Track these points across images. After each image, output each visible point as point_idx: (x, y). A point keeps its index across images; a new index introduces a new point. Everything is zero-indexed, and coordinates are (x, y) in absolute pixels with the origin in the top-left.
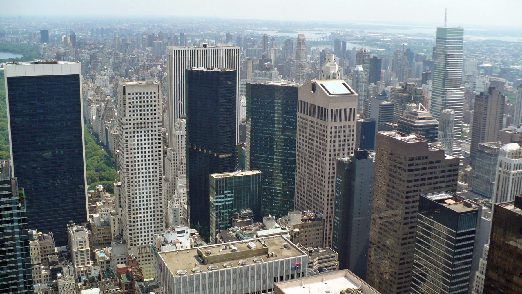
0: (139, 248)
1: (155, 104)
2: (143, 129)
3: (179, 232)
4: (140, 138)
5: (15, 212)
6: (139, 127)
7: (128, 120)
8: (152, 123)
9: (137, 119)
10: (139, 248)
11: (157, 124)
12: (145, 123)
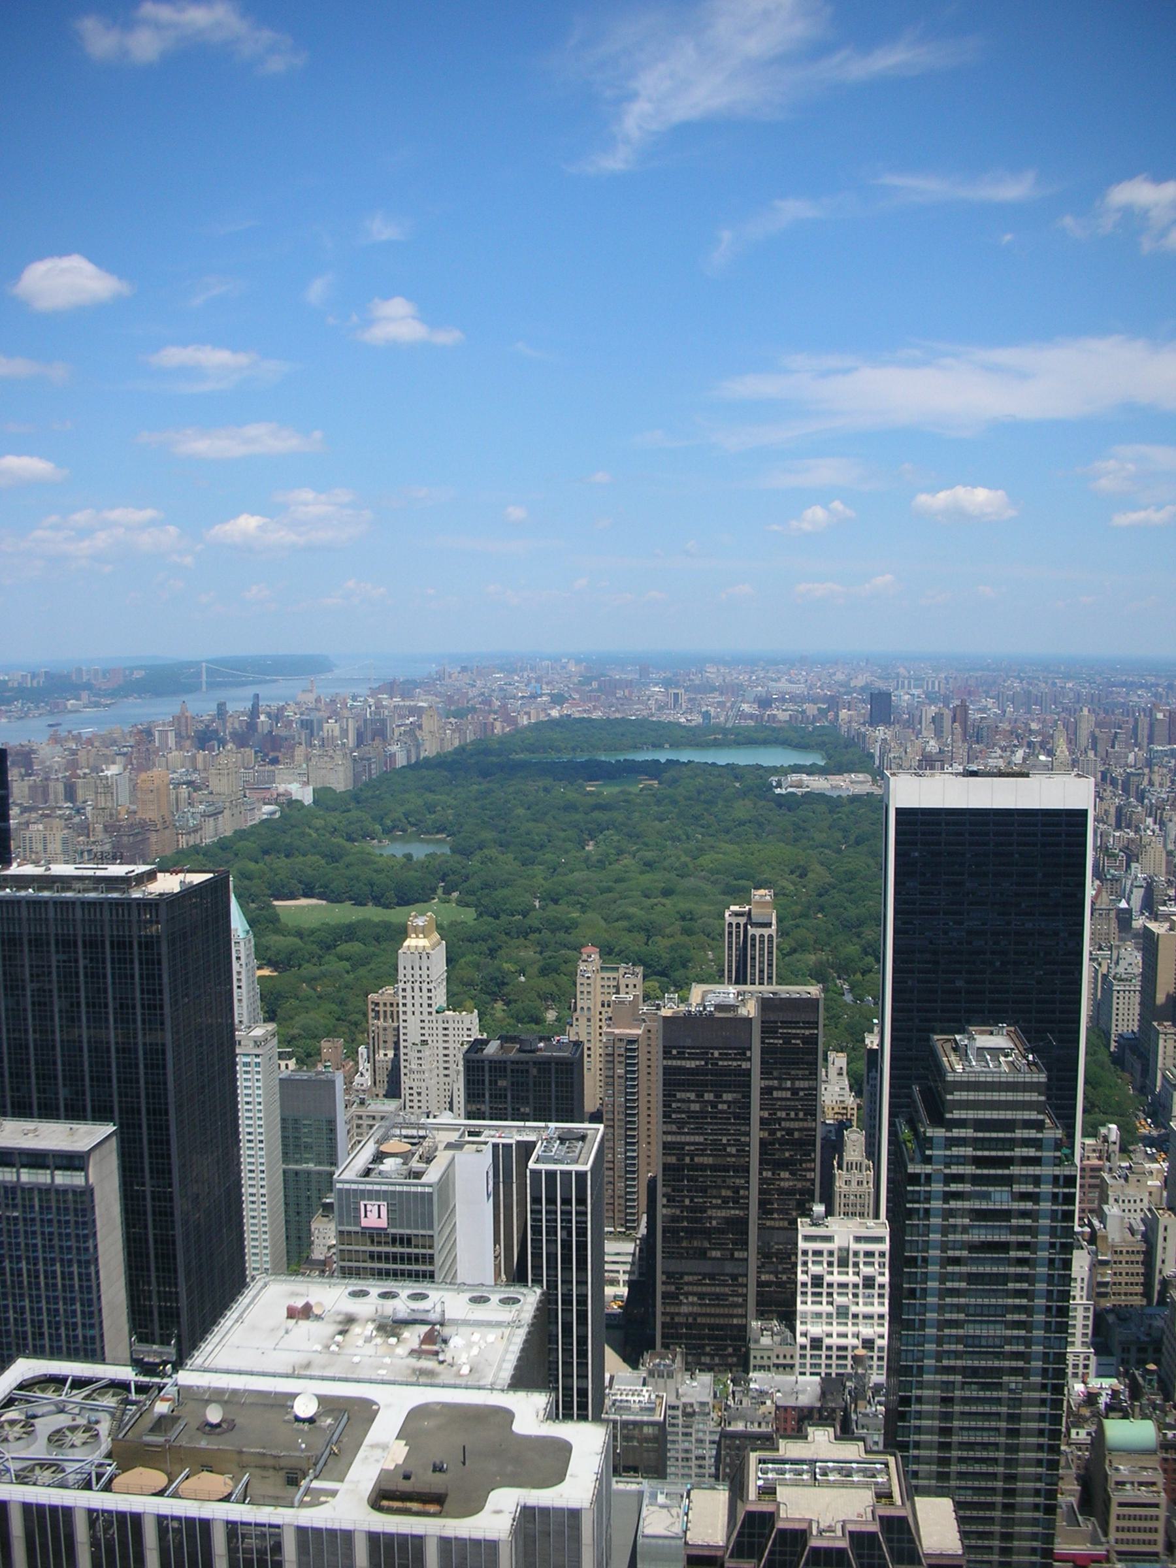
5: (1047, 1171)
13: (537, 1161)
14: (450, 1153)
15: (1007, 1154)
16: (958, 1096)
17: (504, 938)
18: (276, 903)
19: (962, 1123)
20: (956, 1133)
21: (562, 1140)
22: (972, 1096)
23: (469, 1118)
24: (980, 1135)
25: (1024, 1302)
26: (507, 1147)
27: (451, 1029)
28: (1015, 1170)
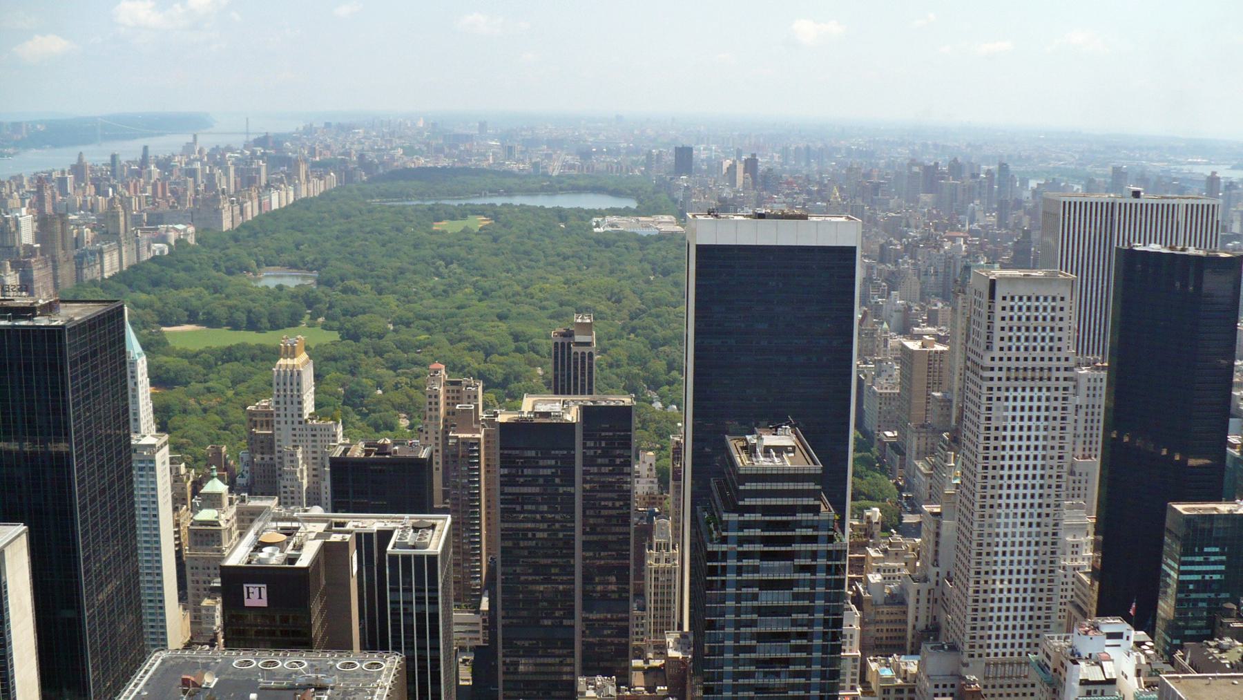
0: (988, 665)
1: (1061, 324)
2: (1029, 384)
3: (1111, 636)
4: (1019, 404)
5: (821, 547)
6: (1021, 376)
7: (997, 359)
8: (1050, 369)
9: (1018, 359)
10: (988, 665)
11: (1062, 374)
12: (1033, 369)
15: (789, 533)
17: (363, 356)
18: (164, 329)
19: (751, 509)
20: (747, 517)
21: (416, 529)
22: (760, 486)
23: (335, 511)
24: (767, 518)
25: (804, 655)
27: (318, 435)
28: (796, 547)
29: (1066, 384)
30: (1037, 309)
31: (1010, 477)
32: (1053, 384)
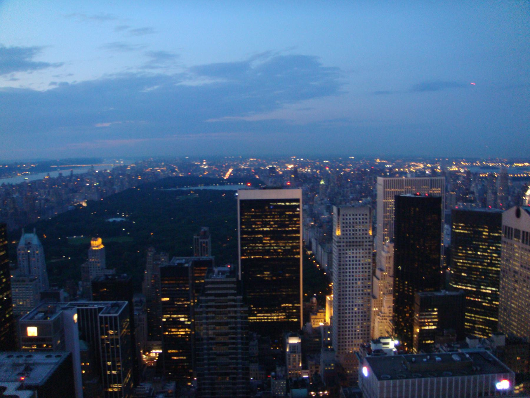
5: (238, 309)
13: (102, 314)
14: (61, 311)
15: (226, 304)
16: (209, 286)
19: (211, 295)
20: (209, 298)
22: (213, 286)
25: (234, 351)
26: (95, 309)
29: (369, 247)
30: (356, 219)
31: (350, 284)
32: (364, 247)
